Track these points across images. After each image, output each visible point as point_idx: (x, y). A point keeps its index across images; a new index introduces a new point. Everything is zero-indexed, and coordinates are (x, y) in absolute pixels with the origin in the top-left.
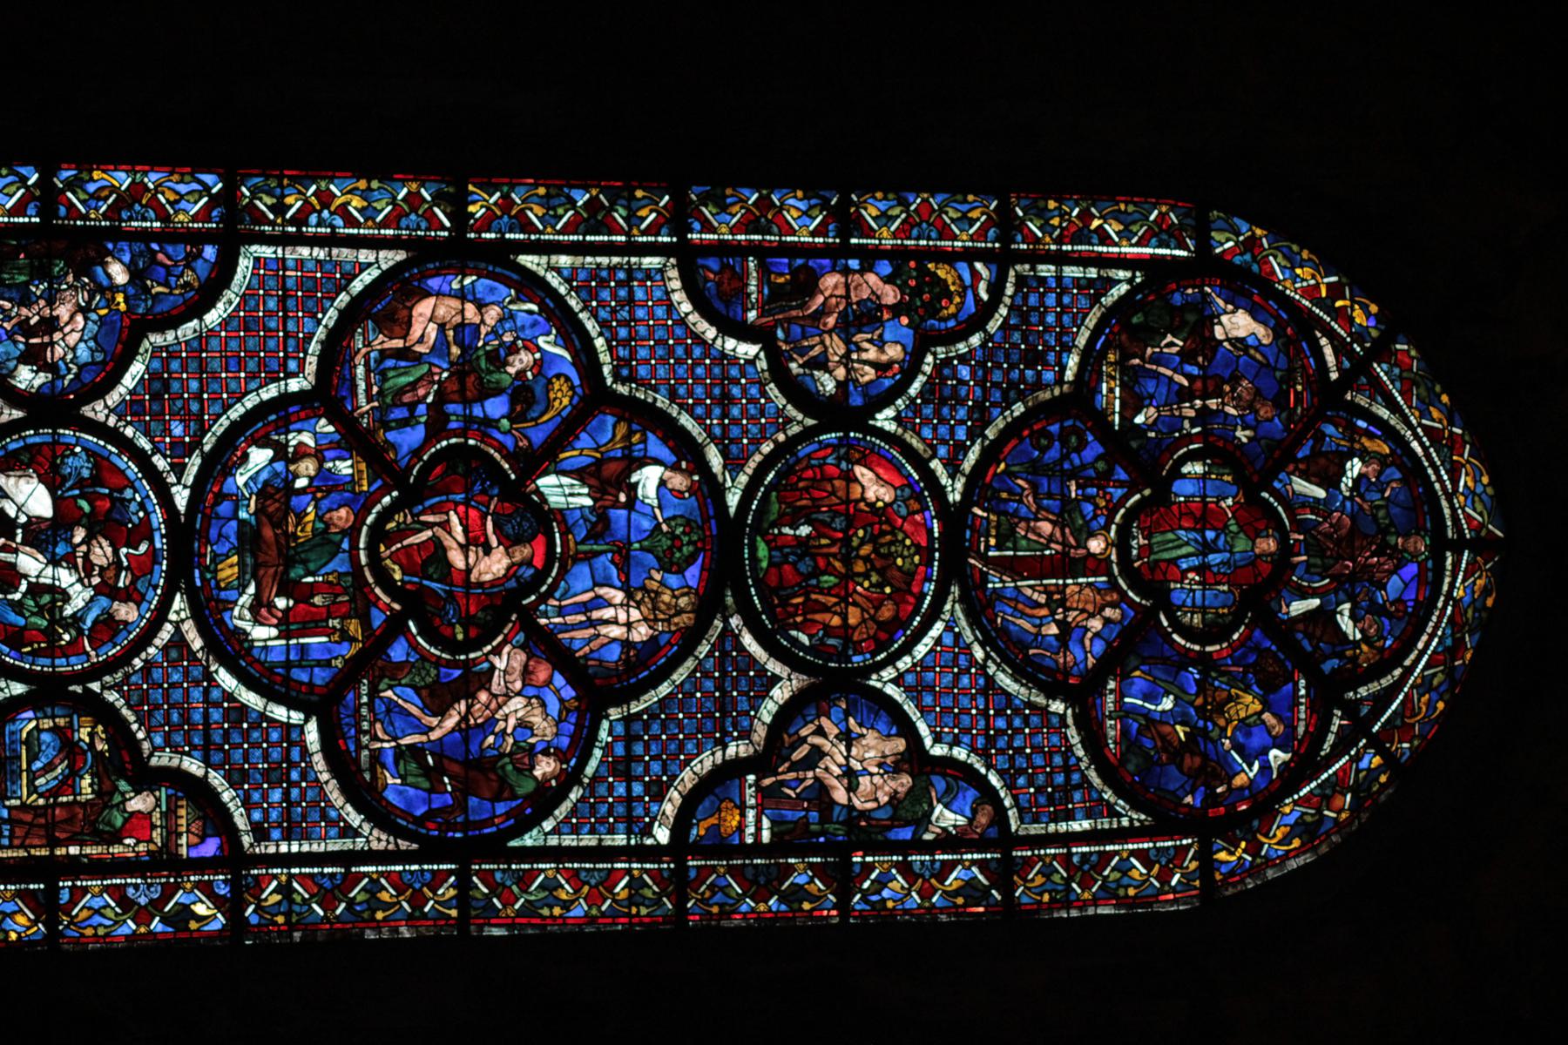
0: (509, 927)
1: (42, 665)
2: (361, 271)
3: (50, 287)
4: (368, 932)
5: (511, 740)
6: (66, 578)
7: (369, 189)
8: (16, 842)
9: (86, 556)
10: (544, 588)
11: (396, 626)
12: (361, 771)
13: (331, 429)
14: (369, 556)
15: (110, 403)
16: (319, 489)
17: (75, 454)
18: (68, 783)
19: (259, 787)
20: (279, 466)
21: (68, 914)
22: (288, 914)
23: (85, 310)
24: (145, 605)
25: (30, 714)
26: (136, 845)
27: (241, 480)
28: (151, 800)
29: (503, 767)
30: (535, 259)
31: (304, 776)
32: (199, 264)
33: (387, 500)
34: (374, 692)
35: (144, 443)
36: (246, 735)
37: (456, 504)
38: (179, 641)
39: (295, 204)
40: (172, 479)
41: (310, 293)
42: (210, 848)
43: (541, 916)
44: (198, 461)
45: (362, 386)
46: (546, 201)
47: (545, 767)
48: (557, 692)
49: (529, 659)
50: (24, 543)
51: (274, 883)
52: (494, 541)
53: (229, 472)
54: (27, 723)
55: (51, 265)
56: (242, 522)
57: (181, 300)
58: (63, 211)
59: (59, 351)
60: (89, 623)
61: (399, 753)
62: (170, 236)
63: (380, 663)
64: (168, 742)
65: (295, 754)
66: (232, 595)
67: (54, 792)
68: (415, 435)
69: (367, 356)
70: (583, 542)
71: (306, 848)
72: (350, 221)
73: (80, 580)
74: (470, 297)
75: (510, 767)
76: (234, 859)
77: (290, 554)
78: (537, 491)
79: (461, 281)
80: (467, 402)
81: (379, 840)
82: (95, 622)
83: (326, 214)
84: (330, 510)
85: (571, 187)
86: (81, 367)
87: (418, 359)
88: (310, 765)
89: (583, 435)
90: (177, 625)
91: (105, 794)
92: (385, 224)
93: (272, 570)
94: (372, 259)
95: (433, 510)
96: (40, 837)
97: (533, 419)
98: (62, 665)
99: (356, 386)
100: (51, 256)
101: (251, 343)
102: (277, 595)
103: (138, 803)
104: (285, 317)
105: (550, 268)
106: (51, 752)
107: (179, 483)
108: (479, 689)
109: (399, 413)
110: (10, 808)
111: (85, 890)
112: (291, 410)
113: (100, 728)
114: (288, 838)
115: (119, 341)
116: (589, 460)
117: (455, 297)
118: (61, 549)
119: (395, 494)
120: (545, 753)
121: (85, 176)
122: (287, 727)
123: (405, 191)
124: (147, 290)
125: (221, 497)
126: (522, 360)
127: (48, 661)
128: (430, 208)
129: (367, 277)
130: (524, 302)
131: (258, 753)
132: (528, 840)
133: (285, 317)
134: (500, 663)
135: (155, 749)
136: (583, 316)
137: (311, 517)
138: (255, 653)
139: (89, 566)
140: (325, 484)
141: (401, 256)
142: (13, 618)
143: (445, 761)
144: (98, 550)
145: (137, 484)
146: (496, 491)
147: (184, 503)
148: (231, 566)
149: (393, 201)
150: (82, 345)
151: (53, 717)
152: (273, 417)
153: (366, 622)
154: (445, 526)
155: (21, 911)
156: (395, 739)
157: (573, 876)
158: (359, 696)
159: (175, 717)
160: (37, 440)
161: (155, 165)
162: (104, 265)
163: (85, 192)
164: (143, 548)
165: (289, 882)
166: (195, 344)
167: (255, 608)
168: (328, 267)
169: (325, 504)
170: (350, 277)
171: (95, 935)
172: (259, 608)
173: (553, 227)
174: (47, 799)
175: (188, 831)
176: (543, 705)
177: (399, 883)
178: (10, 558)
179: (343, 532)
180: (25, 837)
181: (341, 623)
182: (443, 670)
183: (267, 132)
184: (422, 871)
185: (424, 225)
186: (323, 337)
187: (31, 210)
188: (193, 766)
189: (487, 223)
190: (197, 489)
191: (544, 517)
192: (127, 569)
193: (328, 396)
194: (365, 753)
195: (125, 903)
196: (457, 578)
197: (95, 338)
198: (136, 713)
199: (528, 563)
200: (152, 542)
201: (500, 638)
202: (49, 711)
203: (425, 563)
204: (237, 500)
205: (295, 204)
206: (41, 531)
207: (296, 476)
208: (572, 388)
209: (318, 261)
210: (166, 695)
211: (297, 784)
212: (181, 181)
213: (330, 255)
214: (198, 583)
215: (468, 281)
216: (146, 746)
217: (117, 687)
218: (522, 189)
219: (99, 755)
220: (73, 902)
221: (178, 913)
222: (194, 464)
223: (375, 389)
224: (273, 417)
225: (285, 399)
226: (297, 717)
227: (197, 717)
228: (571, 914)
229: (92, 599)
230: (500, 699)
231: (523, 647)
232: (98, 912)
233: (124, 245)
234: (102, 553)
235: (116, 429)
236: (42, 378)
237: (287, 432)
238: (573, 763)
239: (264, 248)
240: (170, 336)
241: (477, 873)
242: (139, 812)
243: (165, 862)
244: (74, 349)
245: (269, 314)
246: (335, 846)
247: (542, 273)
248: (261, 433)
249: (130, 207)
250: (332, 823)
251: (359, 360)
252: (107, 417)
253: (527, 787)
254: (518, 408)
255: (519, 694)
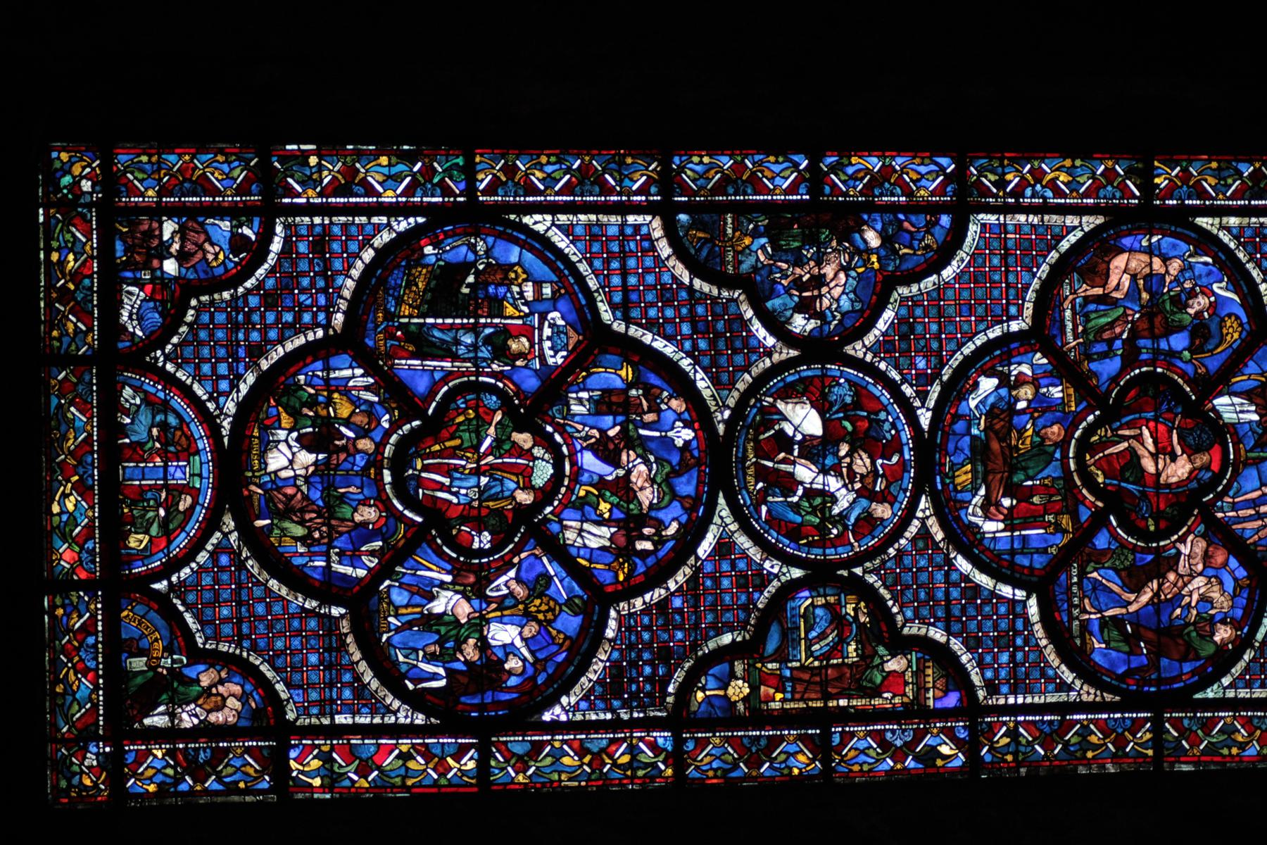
0: (1196, 764)
1: (816, 554)
2: (1068, 233)
3: (818, 251)
4: (1080, 768)
5: (1195, 612)
6: (834, 484)
7: (1073, 166)
8: (797, 696)
9: (850, 466)
10: (1220, 488)
11: (1099, 520)
12: (1073, 638)
13: (1045, 361)
14: (1077, 464)
15: (867, 343)
16: (1036, 410)
17: (840, 385)
18: (837, 648)
19: (990, 651)
20: (1003, 392)
21: (839, 754)
22: (1015, 754)
23: (846, 269)
24: (897, 505)
25: (806, 594)
26: (893, 698)
27: (973, 404)
28: (904, 662)
29: (1189, 634)
30: (1210, 220)
31: (1026, 642)
32: (937, 230)
33: (1091, 418)
34: (1082, 574)
35: (895, 375)
36: (979, 609)
37: (1148, 420)
38: (924, 533)
39: (1013, 180)
40: (917, 403)
41: (1026, 252)
42: (952, 700)
43: (1221, 755)
44: (938, 388)
45: (1069, 326)
46: (1218, 174)
47: (1223, 634)
48: (1232, 572)
49: (1208, 546)
50: (800, 456)
51: (1004, 729)
52: (1179, 450)
53: (963, 397)
54: (804, 601)
55: (819, 233)
56: (974, 438)
57: (923, 260)
58: (827, 189)
59: (826, 302)
60: (852, 520)
61: (1104, 623)
62: (913, 208)
63: (1087, 550)
64: (917, 615)
65: (1019, 624)
66: (967, 496)
67: (827, 656)
68: (1113, 365)
69: (1073, 302)
70: (1251, 450)
71: (1029, 700)
72: (1058, 193)
73: (845, 486)
74: (1157, 252)
75: (1194, 634)
76: (971, 709)
77: (1013, 463)
78: (1214, 409)
79: (1149, 240)
80: (1155, 338)
81: (1089, 694)
82: (857, 519)
83: (1038, 187)
84: (1045, 427)
85: (1238, 161)
86: (843, 315)
87: (1115, 303)
88: (1032, 633)
89: (1251, 363)
90: (923, 521)
91: (867, 657)
92: (1086, 195)
93: (999, 476)
94: (1076, 223)
95: (1129, 425)
96: (816, 692)
97: (1209, 351)
98: (831, 554)
99: (1065, 326)
100: (819, 226)
101: (980, 293)
102: (1003, 496)
103: (894, 665)
104: (1007, 272)
105: (1222, 227)
106: (824, 624)
107: (923, 406)
108: (1168, 571)
109: (1100, 348)
110: (792, 669)
111: (853, 735)
112: (1013, 346)
113: (863, 604)
114: (1014, 692)
115: (873, 293)
116: (1256, 384)
117: (1145, 252)
118: (829, 461)
119: (1097, 413)
120: (1223, 622)
121: (845, 161)
122: (1012, 602)
123: (1103, 167)
124: (896, 252)
125: (957, 417)
126: (1201, 302)
127: (820, 551)
128: (1124, 181)
129: (1073, 238)
130: (1201, 255)
131: (989, 623)
132: (1210, 694)
133: (1007, 272)
134: (1185, 549)
135: (906, 621)
136: (1249, 266)
137: (1030, 433)
138: (986, 543)
139: (852, 475)
140: (1041, 405)
141: (1100, 220)
142: (792, 516)
143: (1141, 630)
144: (859, 462)
145: (889, 408)
146: (1180, 410)
147: (927, 422)
148: (966, 473)
149: (1093, 176)
150: (844, 297)
151: (825, 596)
152: (998, 352)
153: (1075, 517)
154: (1139, 438)
155: (801, 751)
156: (1100, 611)
157: (1247, 722)
158: (1071, 578)
159: (922, 595)
160: (810, 373)
161: (900, 151)
162: (861, 232)
163: (845, 173)
164: (895, 459)
165: (1016, 728)
166: (935, 295)
167: (985, 507)
168: (1041, 230)
169: (1041, 422)
170: (1060, 238)
171: (861, 770)
172: (989, 507)
173: (1224, 194)
174: (821, 661)
175: (934, 687)
176: (1221, 583)
177: (1105, 728)
178: (789, 468)
179: (1056, 445)
180: (805, 692)
181: (1055, 518)
182: (1138, 555)
183: (989, 122)
184: (1124, 718)
185: (1118, 195)
186: (1037, 287)
187: (802, 190)
188: (938, 635)
189: (1169, 192)
190: (938, 412)
191: (1219, 430)
192: (883, 476)
193: (1041, 336)
194: (1076, 623)
195: (885, 745)
196: (1149, 481)
197: (854, 291)
198: (891, 592)
199: (1206, 467)
200: (902, 455)
201: (1185, 529)
202: (821, 590)
203: (1123, 469)
204: (970, 420)
205: (1013, 180)
206: (814, 447)
207: (1017, 400)
208: (1241, 325)
209: (1032, 225)
210: (915, 577)
211: (1021, 649)
212: (922, 164)
213: (1042, 220)
214: (939, 487)
215: (1154, 239)
216: (899, 618)
217: (875, 571)
218: (1198, 164)
219: (862, 626)
220: (843, 744)
221: (927, 753)
222: (935, 391)
223: (1080, 328)
224: (998, 352)
225: (1008, 337)
226: (1020, 594)
227: (940, 595)
228: (1247, 753)
229: (854, 501)
230: (1186, 579)
231: (1203, 536)
232: (863, 752)
233: (877, 216)
234: (862, 464)
235: (872, 363)
236: (812, 324)
237: (1009, 365)
238: (1246, 630)
239: (989, 216)
240: (915, 288)
241: (1169, 720)
242: (894, 671)
243: (916, 712)
244: (838, 300)
245: (994, 269)
246: (1052, 698)
247: (1215, 231)
248: (989, 365)
249: (881, 185)
250: (1050, 680)
251: (1067, 304)
252: (865, 354)
253: (1210, 649)
254: (1197, 342)
255: (1201, 574)
